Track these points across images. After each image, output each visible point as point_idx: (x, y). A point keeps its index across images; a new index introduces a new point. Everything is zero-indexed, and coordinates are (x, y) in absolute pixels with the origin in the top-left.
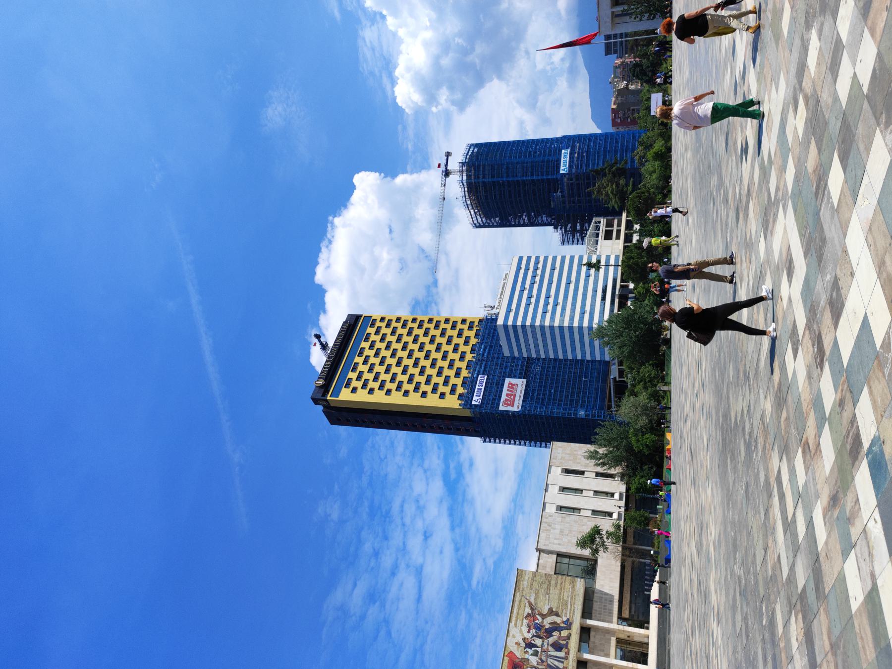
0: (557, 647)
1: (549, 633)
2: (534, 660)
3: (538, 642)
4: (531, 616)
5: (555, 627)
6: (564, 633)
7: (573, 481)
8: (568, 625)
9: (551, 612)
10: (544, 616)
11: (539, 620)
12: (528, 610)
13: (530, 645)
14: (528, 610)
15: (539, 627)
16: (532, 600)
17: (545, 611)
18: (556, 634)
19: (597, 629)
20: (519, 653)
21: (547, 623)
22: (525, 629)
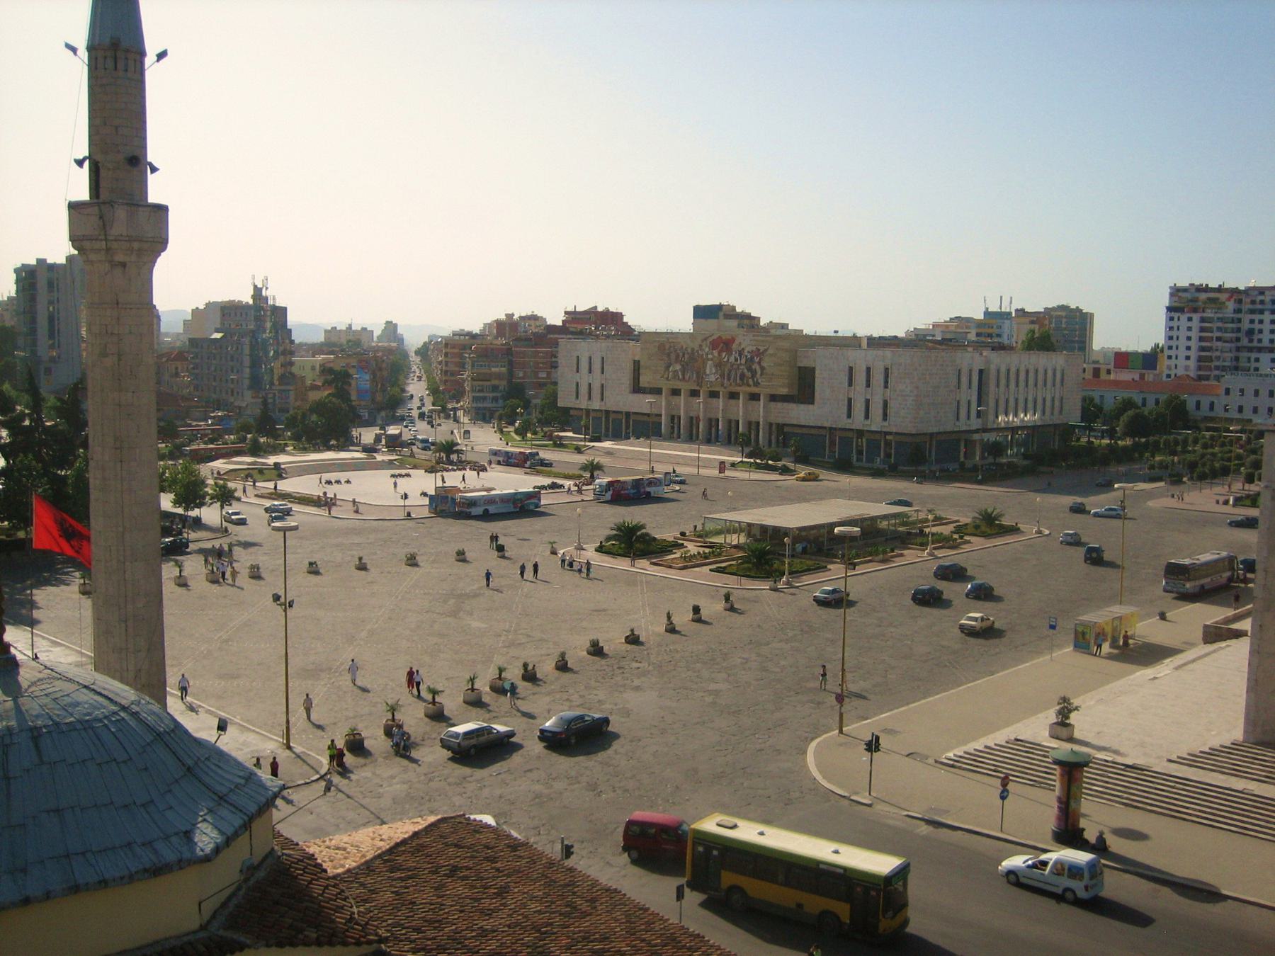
1: (749, 369)
2: (732, 359)
3: (743, 361)
4: (759, 353)
5: (754, 373)
6: (751, 381)
7: (878, 378)
8: (757, 384)
9: (762, 369)
10: (759, 363)
11: (757, 360)
12: (762, 349)
13: (740, 355)
14: (762, 349)
16: (770, 351)
17: (764, 364)
18: (749, 374)
19: (686, 412)
20: (734, 346)
21: (756, 367)
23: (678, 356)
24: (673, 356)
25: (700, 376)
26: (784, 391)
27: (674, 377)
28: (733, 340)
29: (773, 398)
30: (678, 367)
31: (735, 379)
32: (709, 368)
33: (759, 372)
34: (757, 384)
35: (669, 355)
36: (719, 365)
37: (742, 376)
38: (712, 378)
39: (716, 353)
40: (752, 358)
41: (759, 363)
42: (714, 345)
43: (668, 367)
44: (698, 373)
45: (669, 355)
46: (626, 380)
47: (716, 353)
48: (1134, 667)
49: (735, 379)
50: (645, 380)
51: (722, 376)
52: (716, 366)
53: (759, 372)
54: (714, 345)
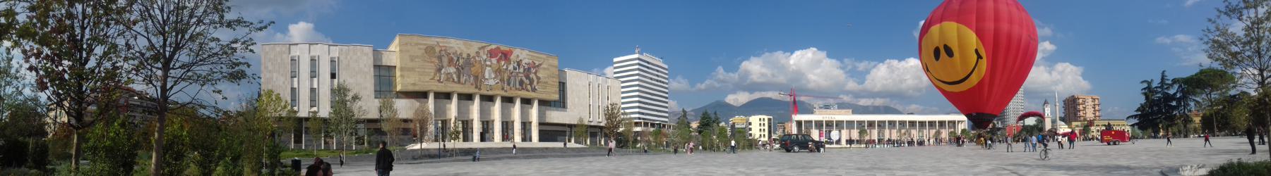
0: (521, 83)
1: (527, 77)
2: (511, 67)
4: (535, 66)
5: (531, 82)
8: (534, 90)
9: (538, 78)
21: (532, 76)
22: (527, 61)
23: (451, 60)
24: (445, 60)
25: (478, 80)
27: (448, 80)
29: (544, 103)
30: (452, 70)
32: (488, 73)
34: (534, 90)
35: (440, 58)
36: (498, 71)
37: (521, 83)
38: (492, 82)
39: (494, 61)
42: (492, 54)
43: (439, 70)
44: (476, 77)
45: (440, 58)
47: (494, 61)
48: (955, 109)
52: (495, 72)
54: (492, 54)
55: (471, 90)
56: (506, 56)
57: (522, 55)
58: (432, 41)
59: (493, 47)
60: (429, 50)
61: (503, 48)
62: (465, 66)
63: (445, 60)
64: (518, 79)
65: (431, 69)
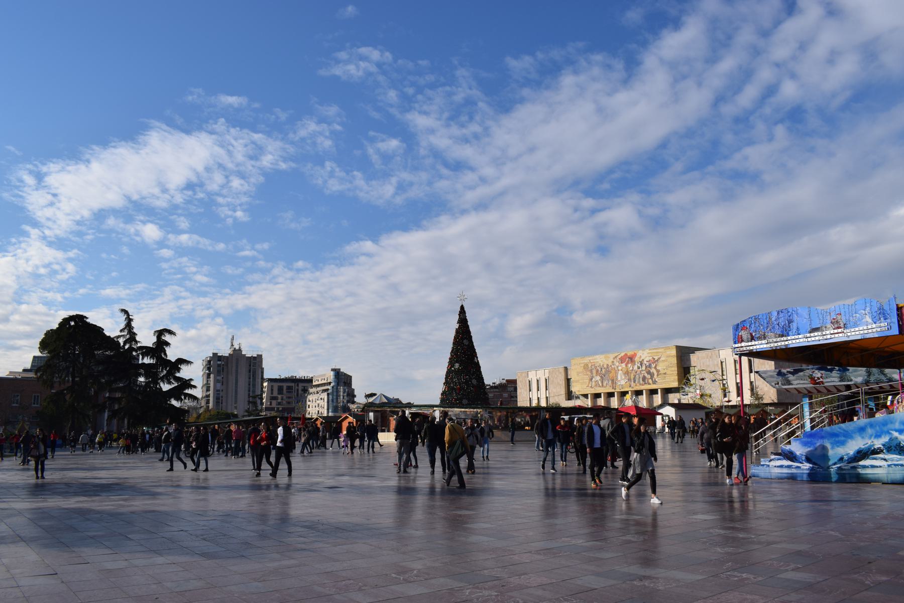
0: (644, 378)
1: (649, 373)
2: (636, 368)
3: (644, 368)
5: (652, 375)
6: (650, 381)
8: (655, 382)
9: (658, 371)
10: (655, 368)
11: (653, 366)
12: (656, 358)
14: (656, 358)
15: (650, 366)
18: (649, 376)
20: (637, 359)
21: (653, 370)
22: (647, 359)
23: (597, 371)
24: (594, 372)
26: (675, 384)
28: (635, 355)
29: (667, 391)
30: (598, 378)
31: (639, 382)
32: (620, 376)
33: (656, 374)
34: (655, 382)
35: (591, 371)
36: (627, 373)
37: (644, 378)
38: (623, 382)
40: (650, 366)
41: (655, 368)
42: (622, 360)
44: (613, 381)
45: (591, 371)
46: (563, 391)
47: (623, 365)
49: (639, 382)
50: (576, 389)
51: (629, 380)
53: (656, 374)
54: (622, 360)
55: (611, 390)
56: (631, 359)
57: (644, 355)
58: (586, 360)
59: (622, 354)
60: (586, 367)
61: (630, 353)
62: (606, 373)
63: (594, 372)
64: (641, 376)
65: (587, 378)
